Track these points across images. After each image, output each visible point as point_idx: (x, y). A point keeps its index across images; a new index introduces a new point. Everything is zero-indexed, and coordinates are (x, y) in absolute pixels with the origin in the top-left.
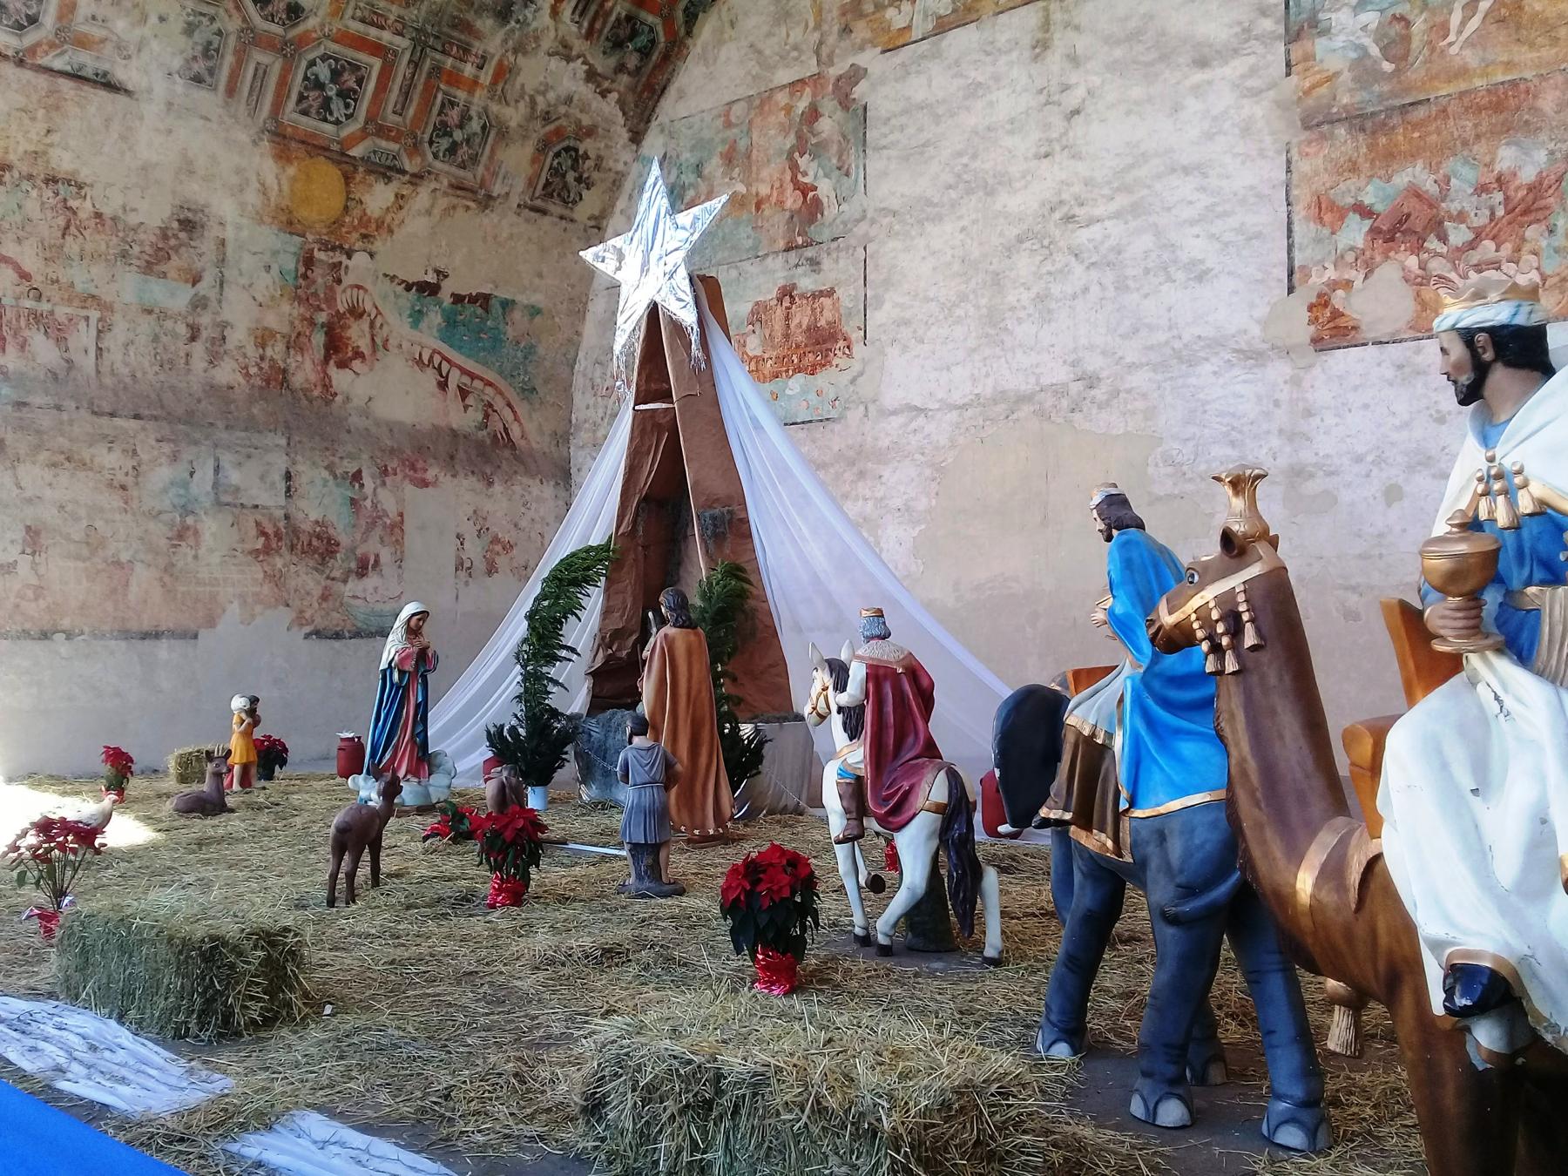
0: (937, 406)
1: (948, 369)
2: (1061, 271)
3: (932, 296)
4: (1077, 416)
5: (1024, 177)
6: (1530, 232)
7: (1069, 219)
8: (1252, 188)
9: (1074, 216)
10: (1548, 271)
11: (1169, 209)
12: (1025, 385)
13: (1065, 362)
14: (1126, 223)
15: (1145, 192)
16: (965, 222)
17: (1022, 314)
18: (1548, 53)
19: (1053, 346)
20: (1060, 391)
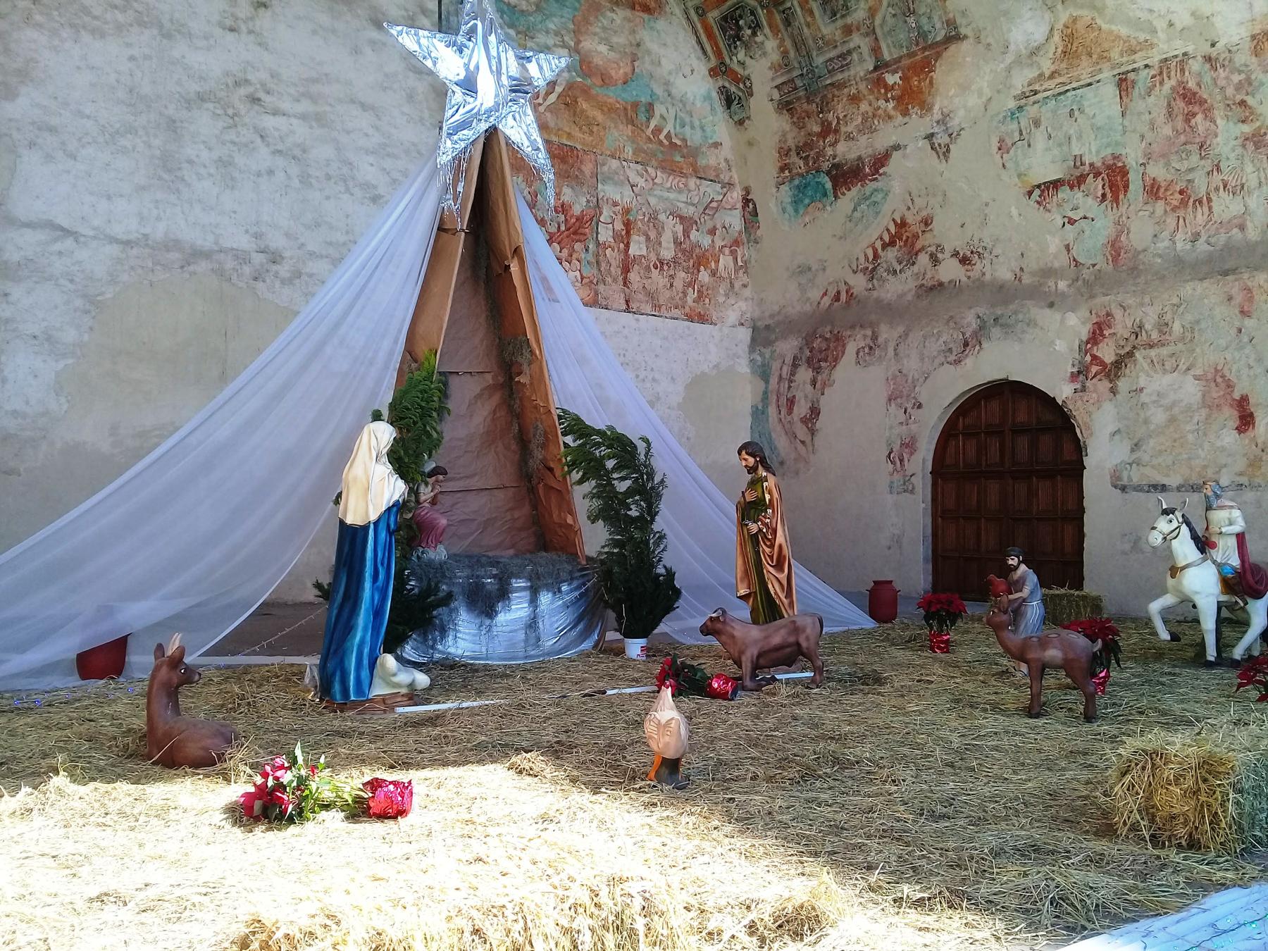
0: (91, 233)
1: (109, 198)
2: (246, 145)
3: (87, 112)
4: (260, 285)
5: (206, 38)
6: (578, 246)
7: (255, 100)
8: (414, 144)
9: (259, 100)
10: (584, 275)
11: (348, 133)
12: (207, 242)
13: (247, 231)
14: (311, 127)
15: (328, 108)
16: (135, 52)
17: (202, 171)
18: (589, 139)
19: (235, 212)
20: (241, 257)
